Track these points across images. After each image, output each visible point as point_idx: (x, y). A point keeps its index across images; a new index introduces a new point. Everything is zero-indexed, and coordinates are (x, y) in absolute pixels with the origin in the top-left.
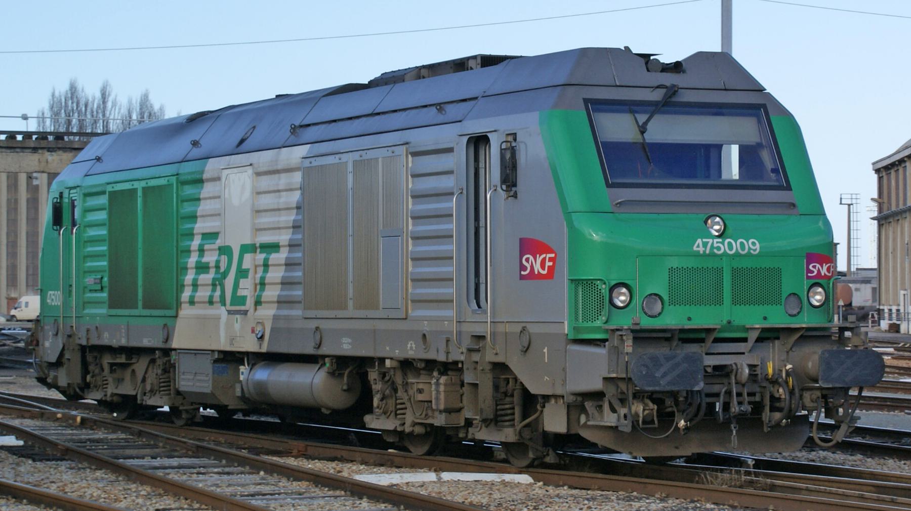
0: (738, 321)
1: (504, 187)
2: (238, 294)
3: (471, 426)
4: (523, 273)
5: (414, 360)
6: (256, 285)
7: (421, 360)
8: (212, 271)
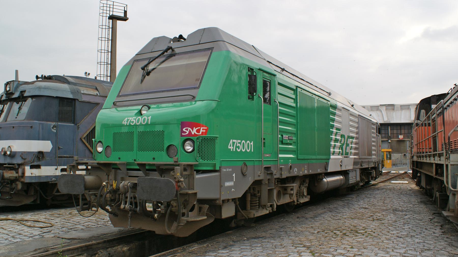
8: (339, 142)
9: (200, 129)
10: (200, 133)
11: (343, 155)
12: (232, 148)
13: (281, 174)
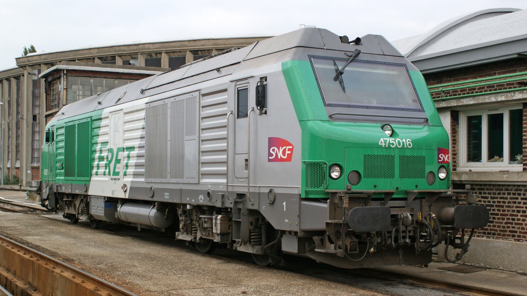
0: (403, 188)
1: (259, 108)
2: (116, 171)
3: (235, 243)
4: (270, 158)
5: (203, 205)
6: (124, 166)
7: (207, 206)
8: (105, 160)
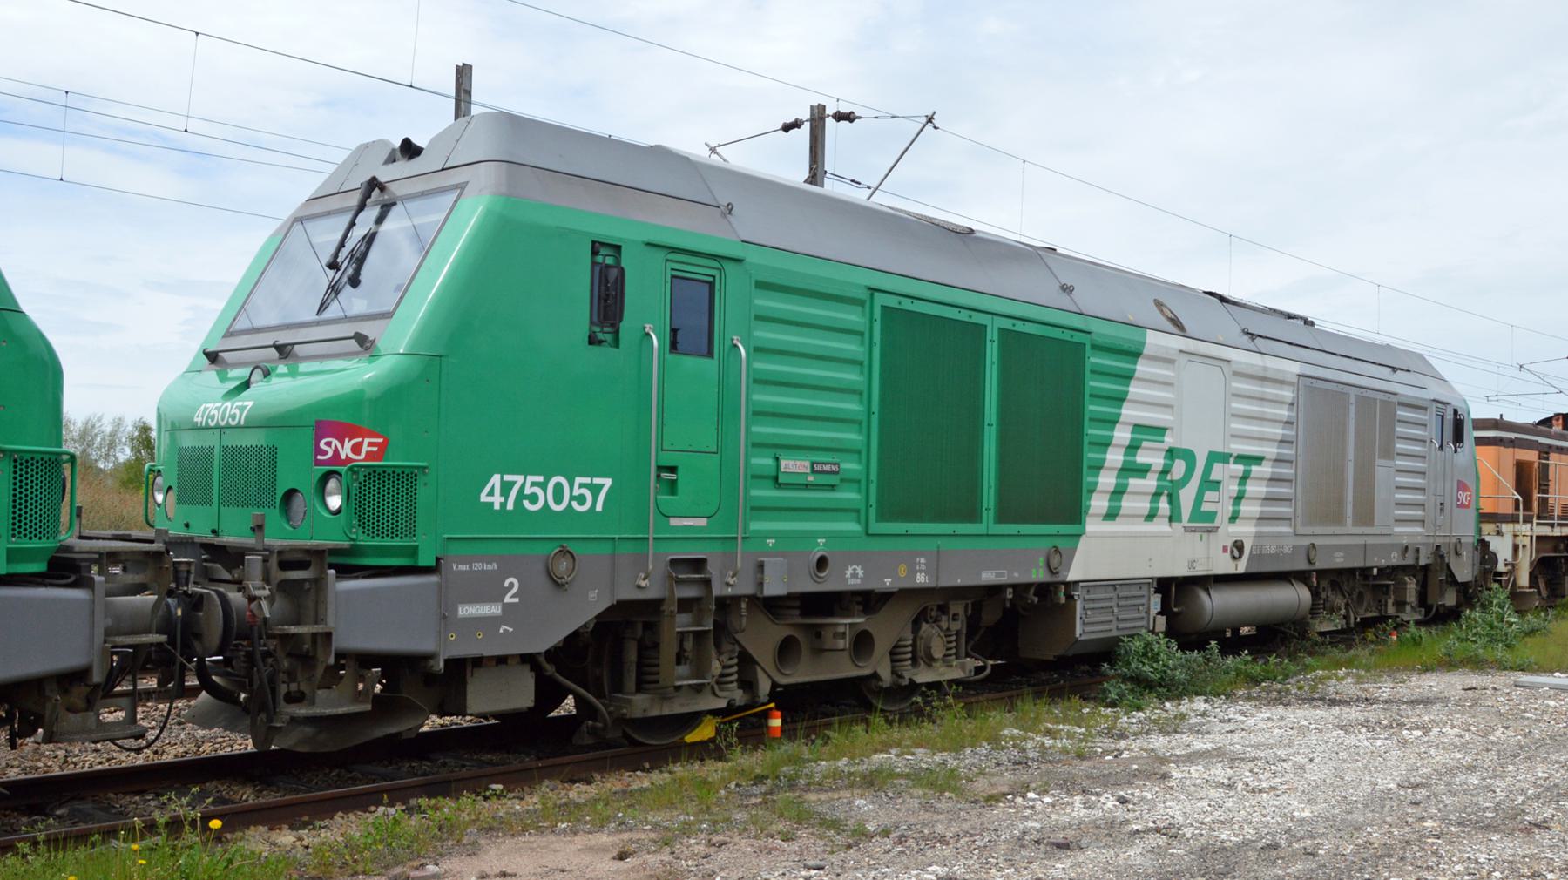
9: (363, 442)
10: (363, 456)
11: (1180, 520)
12: (497, 500)
13: (761, 584)
